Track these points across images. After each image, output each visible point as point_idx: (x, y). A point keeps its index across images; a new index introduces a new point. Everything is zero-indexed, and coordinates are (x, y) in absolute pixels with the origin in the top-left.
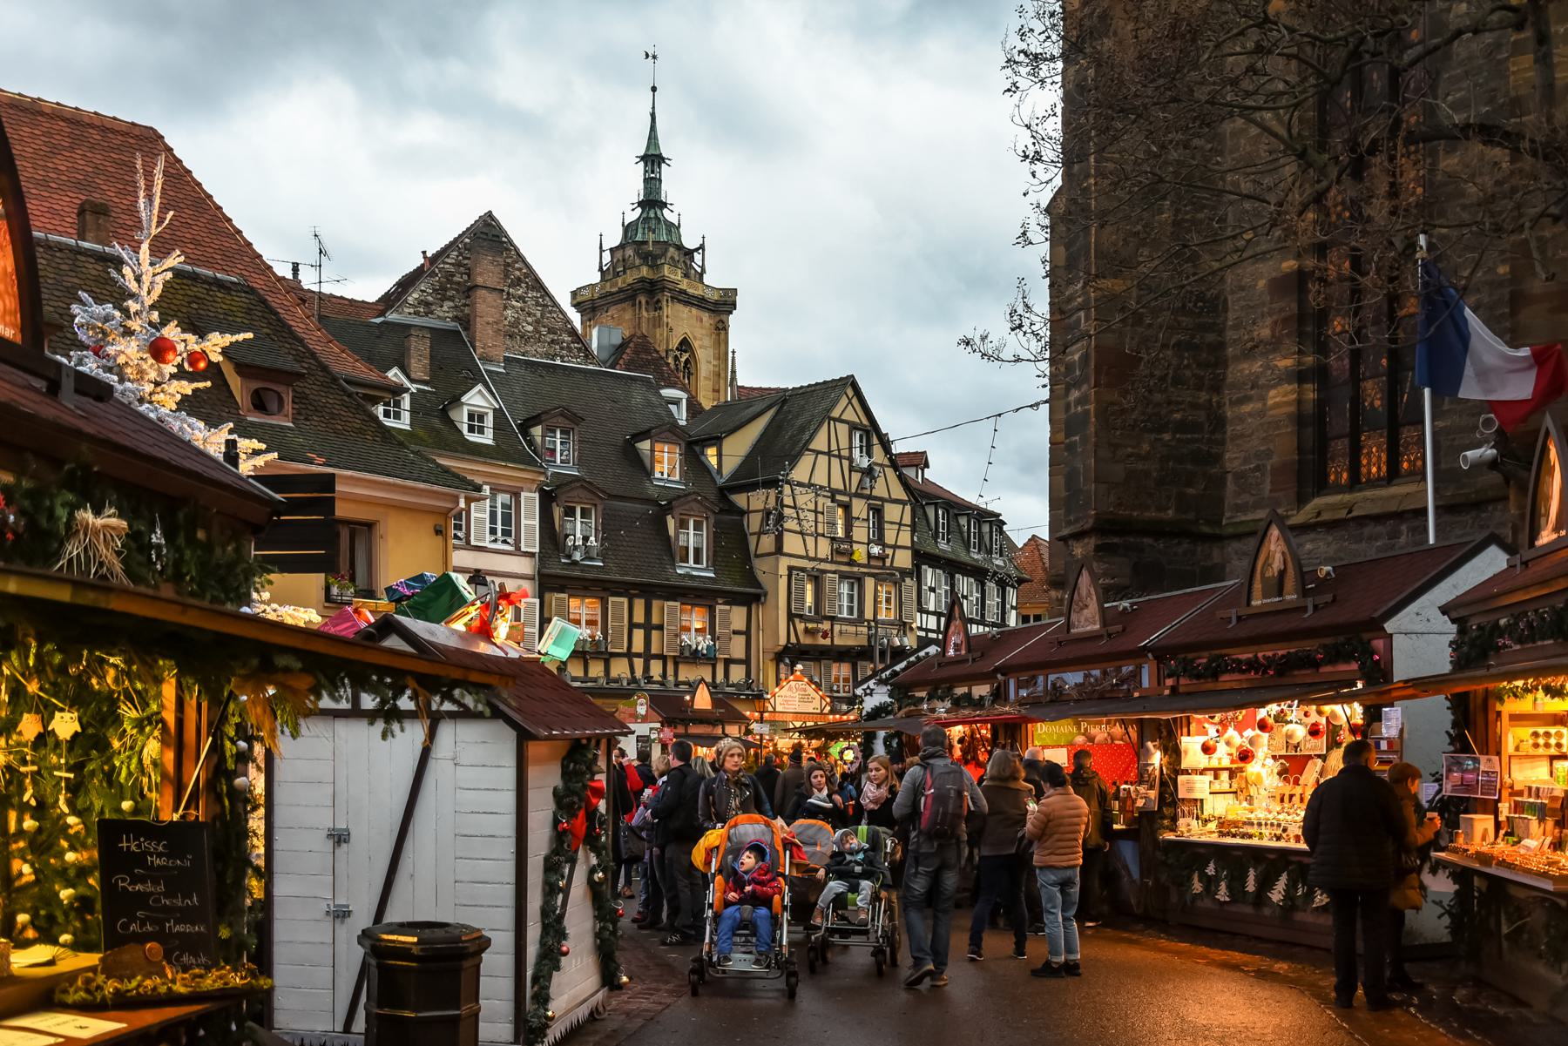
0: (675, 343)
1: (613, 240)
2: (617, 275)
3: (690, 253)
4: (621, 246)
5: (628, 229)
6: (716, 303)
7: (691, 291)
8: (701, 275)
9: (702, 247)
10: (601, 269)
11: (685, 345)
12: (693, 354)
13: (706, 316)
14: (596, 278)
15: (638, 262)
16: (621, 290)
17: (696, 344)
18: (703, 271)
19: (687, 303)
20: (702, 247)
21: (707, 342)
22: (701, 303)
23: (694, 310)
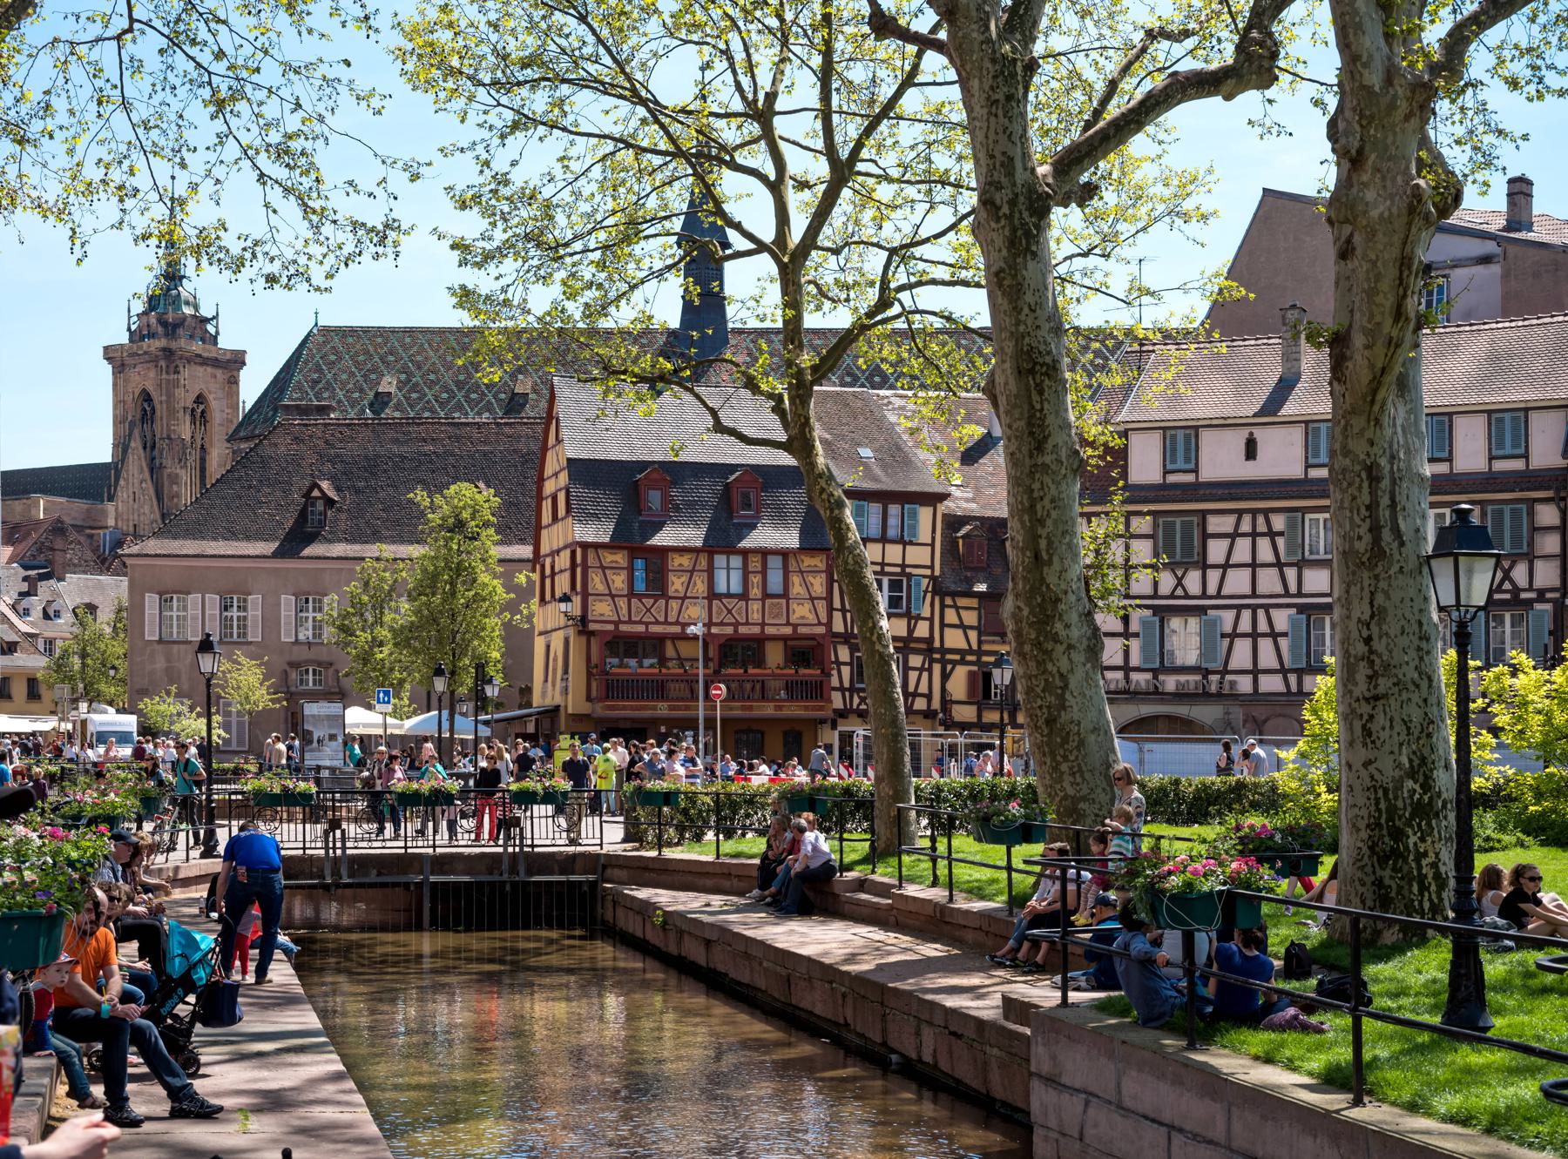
0: (193, 397)
1: (138, 307)
2: (142, 338)
3: (207, 320)
4: (145, 313)
5: (153, 302)
6: (229, 361)
7: (205, 355)
8: (215, 338)
9: (215, 317)
10: (129, 329)
11: (200, 399)
12: (207, 406)
13: (219, 373)
14: (124, 338)
15: (160, 330)
16: (146, 353)
17: (211, 397)
18: (217, 333)
19: (202, 364)
20: (215, 317)
21: (220, 395)
22: (215, 363)
23: (209, 369)
